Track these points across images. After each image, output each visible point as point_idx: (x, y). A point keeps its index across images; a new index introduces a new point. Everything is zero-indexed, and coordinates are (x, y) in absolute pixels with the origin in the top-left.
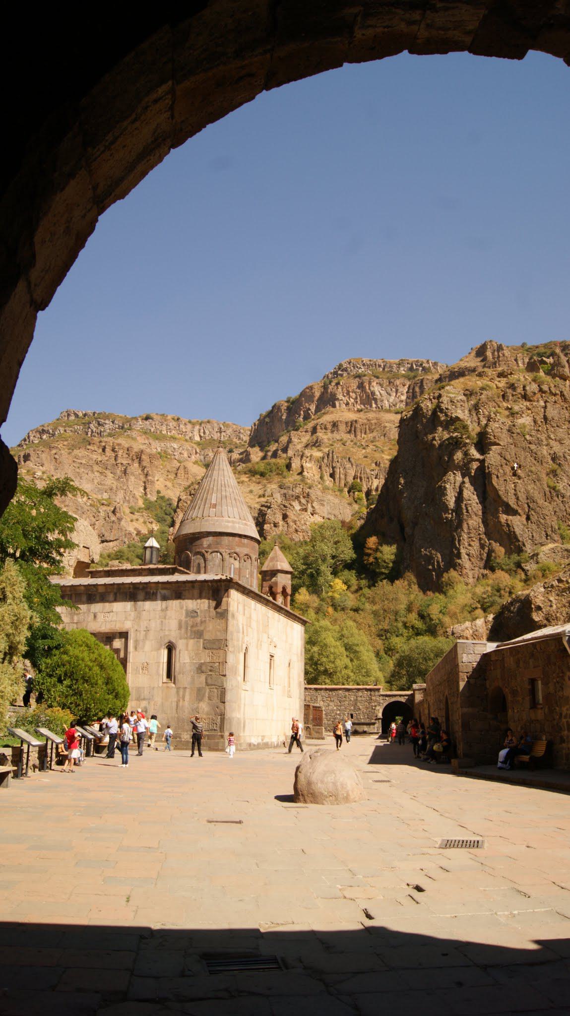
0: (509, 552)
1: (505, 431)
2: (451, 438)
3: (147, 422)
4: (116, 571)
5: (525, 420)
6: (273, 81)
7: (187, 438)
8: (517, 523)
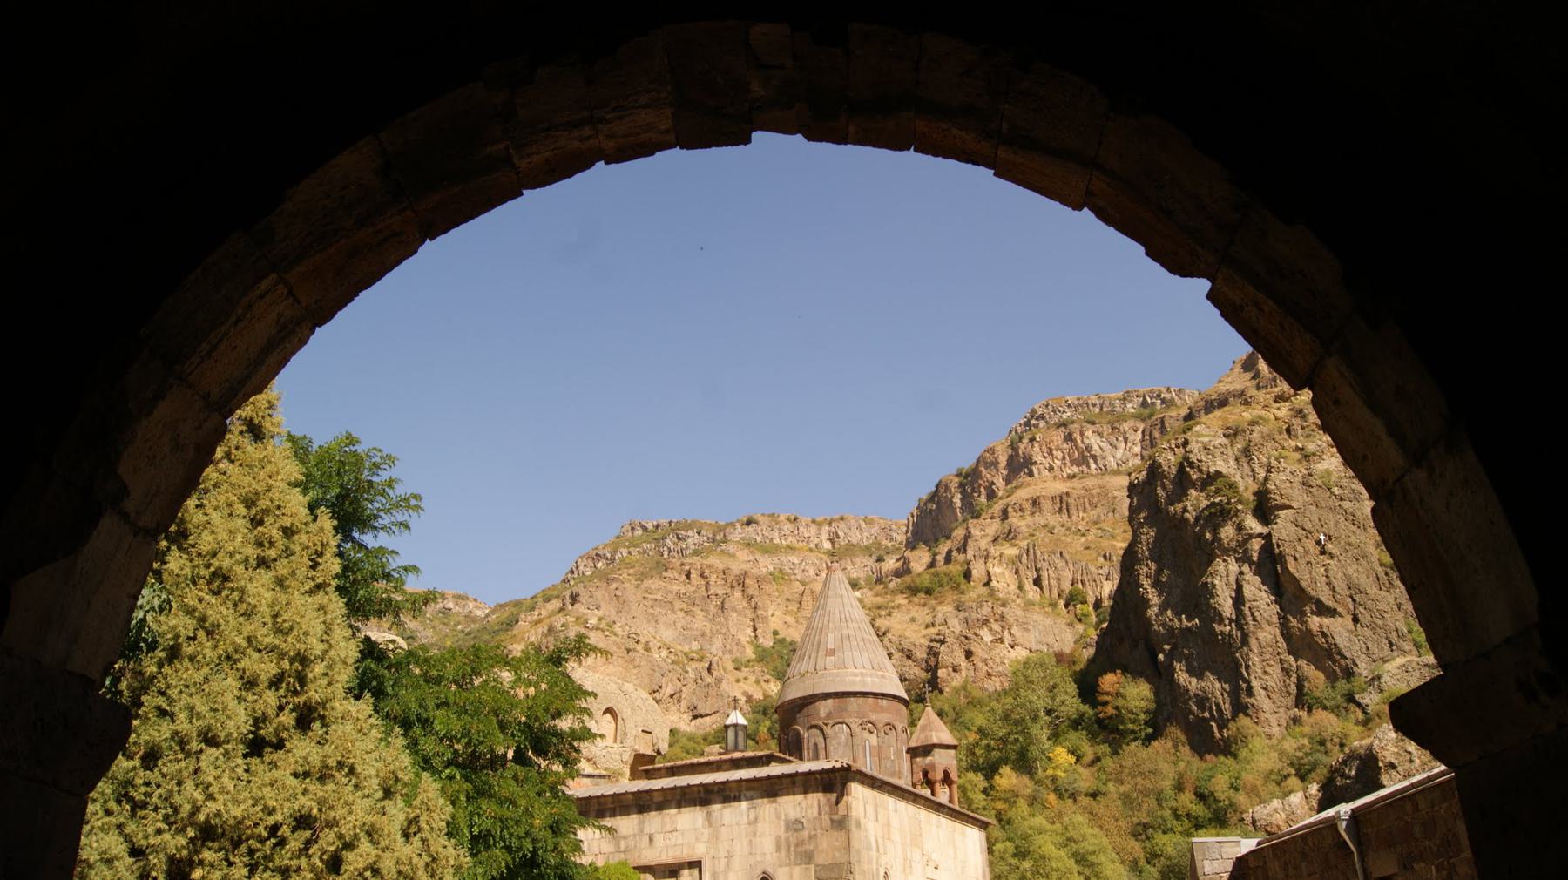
0: (1332, 678)
1: (1297, 485)
2: (1213, 504)
3: (750, 529)
4: (683, 766)
6: (434, 229)
7: (812, 546)
8: (1339, 629)
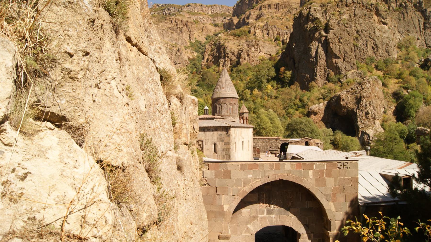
0: (335, 74)
1: (336, 23)
5: (346, 17)
7: (206, 13)
8: (339, 62)
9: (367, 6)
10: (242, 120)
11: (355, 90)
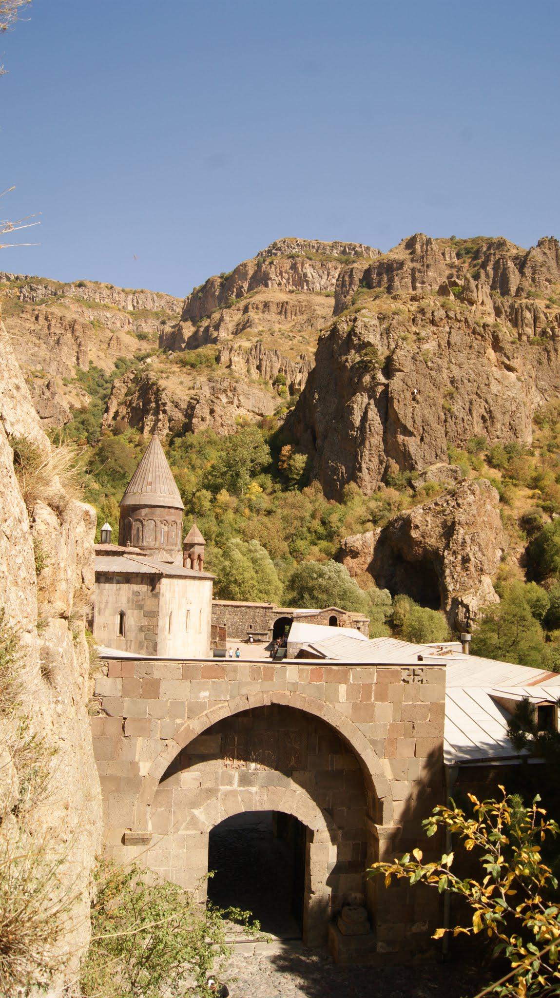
0: (403, 469)
1: (409, 359)
3: (81, 290)
5: (430, 346)
7: (121, 307)
8: (412, 444)
9: (475, 328)
10: (189, 561)
11: (442, 506)
